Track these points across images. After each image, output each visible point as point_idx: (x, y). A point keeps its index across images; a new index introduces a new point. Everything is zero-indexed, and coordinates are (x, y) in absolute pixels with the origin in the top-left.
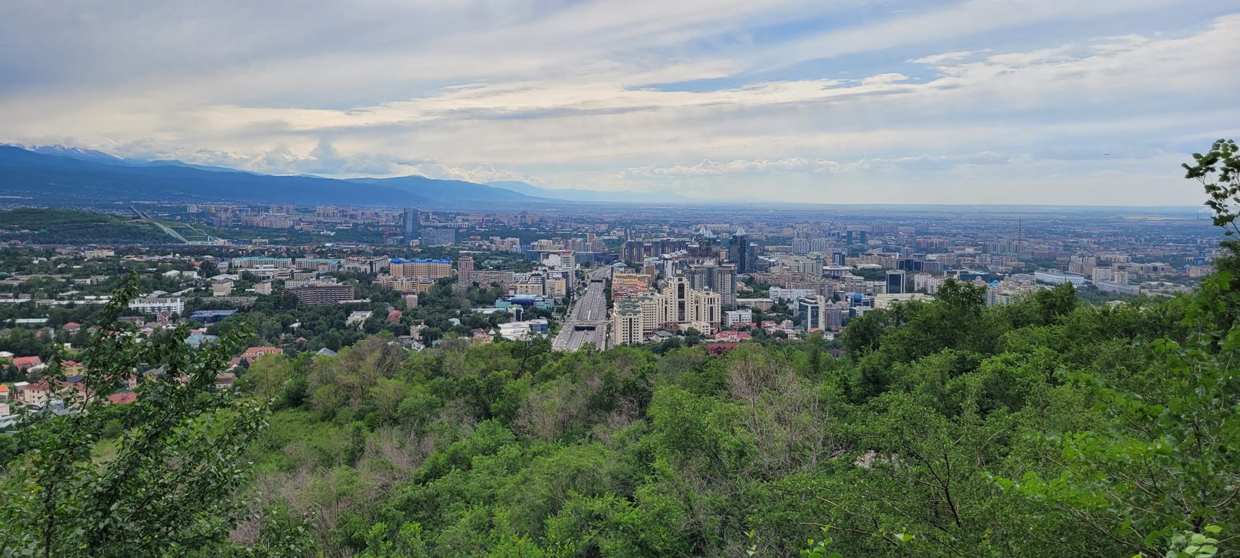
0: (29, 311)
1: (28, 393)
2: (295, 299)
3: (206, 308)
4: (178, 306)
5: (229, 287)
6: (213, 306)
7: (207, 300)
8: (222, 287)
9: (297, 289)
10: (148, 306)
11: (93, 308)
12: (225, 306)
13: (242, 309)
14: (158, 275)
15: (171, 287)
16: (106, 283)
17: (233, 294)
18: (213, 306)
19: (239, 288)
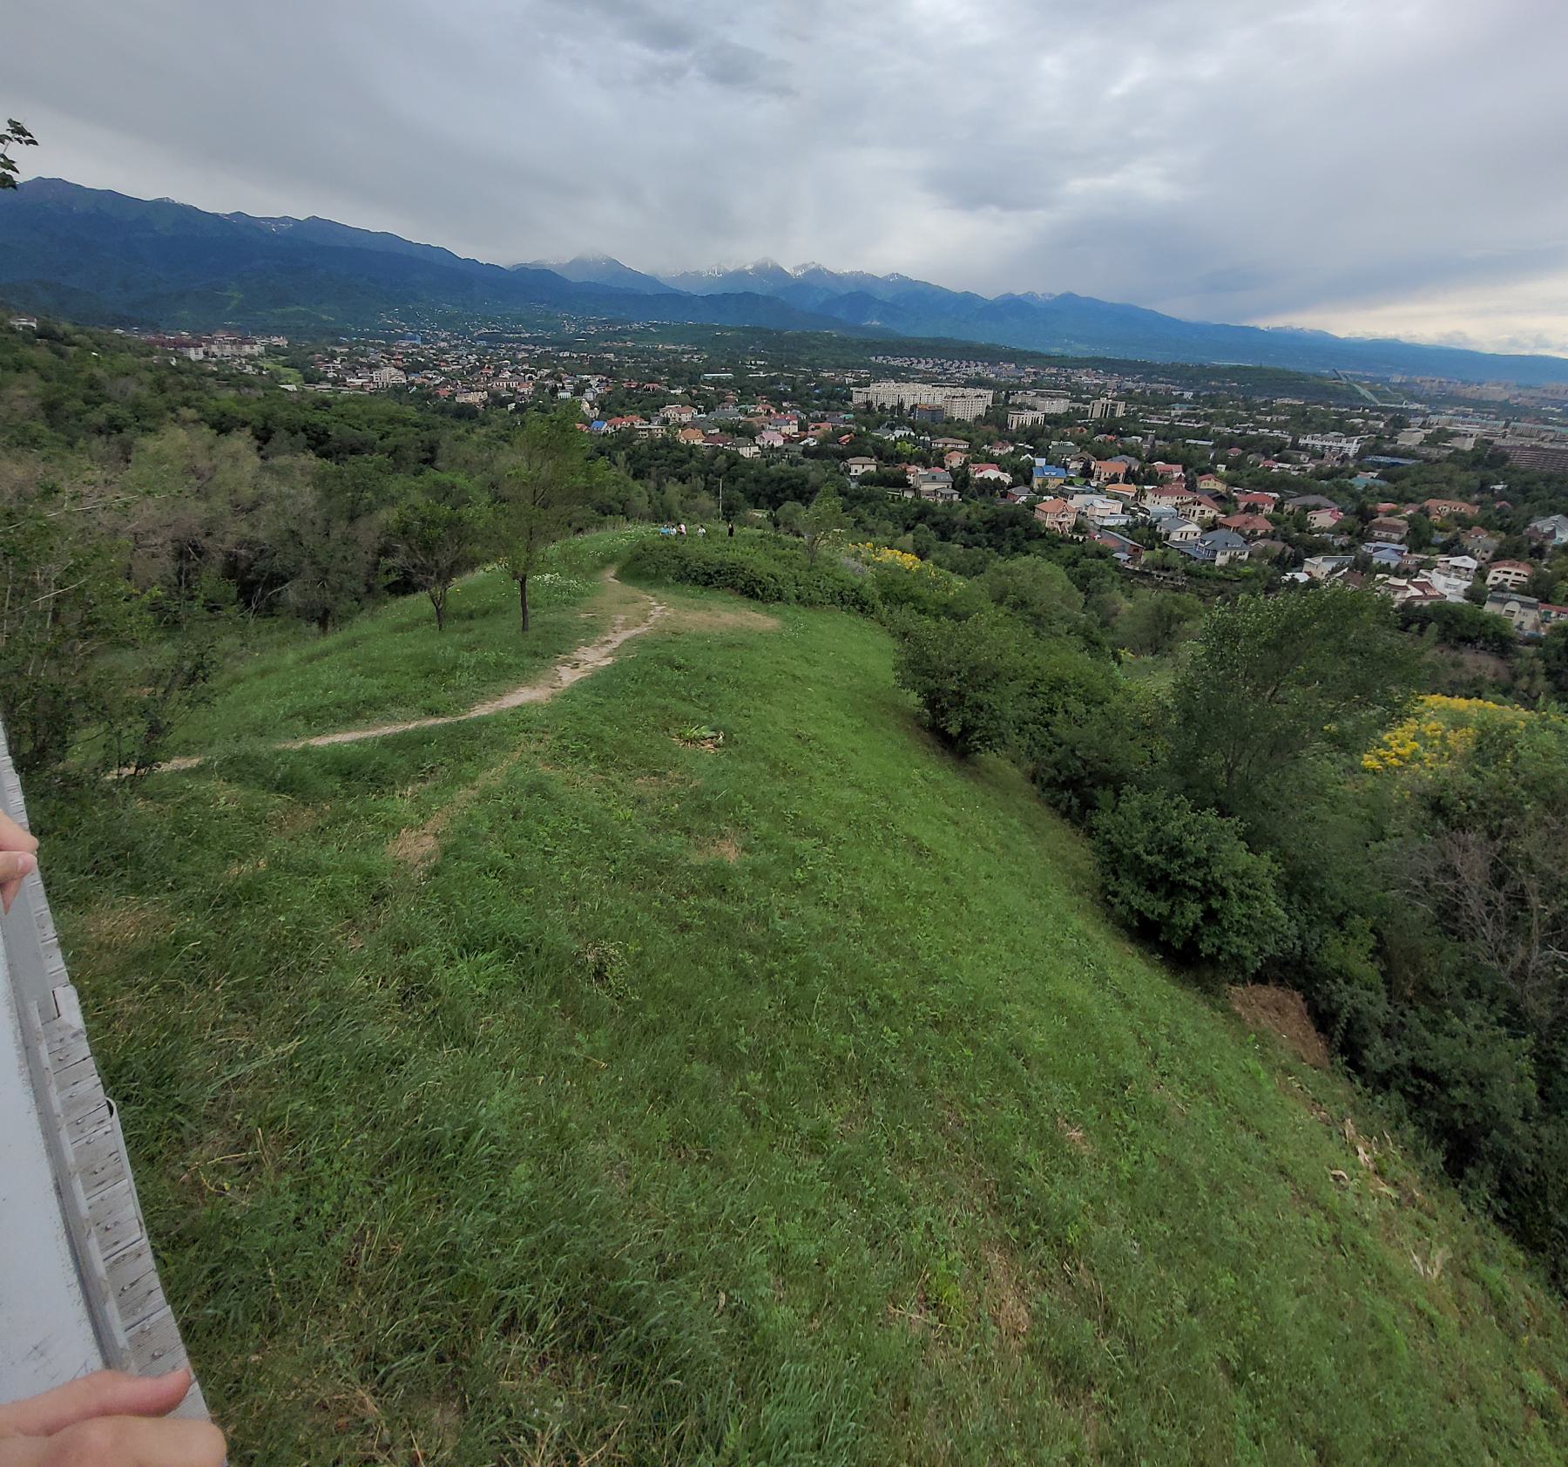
0: (1203, 434)
1: (1150, 496)
2: (1505, 458)
3: (1383, 455)
4: (1352, 447)
5: (1419, 436)
6: (1393, 453)
7: (1387, 447)
8: (1411, 438)
9: (1512, 447)
10: (1318, 443)
11: (1261, 438)
12: (1409, 454)
13: (1427, 460)
14: (1340, 422)
15: (1352, 432)
16: (1286, 422)
17: (1421, 444)
18: (1393, 453)
19: (1431, 441)
